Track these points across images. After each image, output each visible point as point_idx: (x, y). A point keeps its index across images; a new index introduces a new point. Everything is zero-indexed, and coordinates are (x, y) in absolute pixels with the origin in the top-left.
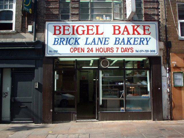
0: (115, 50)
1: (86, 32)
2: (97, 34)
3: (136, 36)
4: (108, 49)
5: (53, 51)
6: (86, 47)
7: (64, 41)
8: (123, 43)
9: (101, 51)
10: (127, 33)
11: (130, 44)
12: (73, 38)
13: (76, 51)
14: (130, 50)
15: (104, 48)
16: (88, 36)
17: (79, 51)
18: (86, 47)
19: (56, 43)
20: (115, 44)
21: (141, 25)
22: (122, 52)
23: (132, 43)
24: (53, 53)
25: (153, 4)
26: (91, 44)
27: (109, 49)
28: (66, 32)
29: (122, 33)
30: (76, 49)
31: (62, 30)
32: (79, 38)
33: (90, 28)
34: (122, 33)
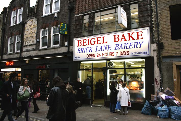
0: (115, 54)
1: (96, 43)
2: (103, 43)
3: (132, 41)
4: (110, 54)
7: (137, 44)
8: (121, 48)
9: (106, 55)
10: (124, 40)
11: (127, 48)
14: (126, 53)
16: (97, 45)
17: (92, 56)
18: (96, 53)
19: (79, 52)
20: (116, 49)
22: (120, 55)
23: (128, 47)
25: (147, 13)
26: (99, 51)
28: (85, 44)
29: (120, 40)
30: (90, 55)
31: (82, 43)
33: (99, 39)
34: (120, 40)
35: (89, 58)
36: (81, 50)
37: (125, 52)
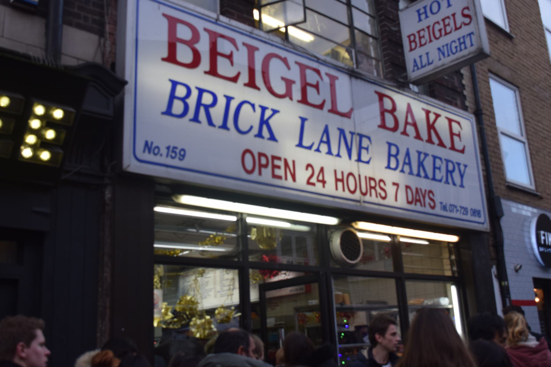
5: (164, 151)
6: (301, 157)
12: (253, 106)
13: (263, 170)
14: (427, 200)
15: (359, 176)
17: (278, 172)
18: (301, 157)
21: (444, 114)
24: (163, 160)
26: (318, 150)
27: (373, 184)
28: (223, 66)
32: (275, 112)
35: (255, 176)
36: (199, 103)
37: (421, 190)
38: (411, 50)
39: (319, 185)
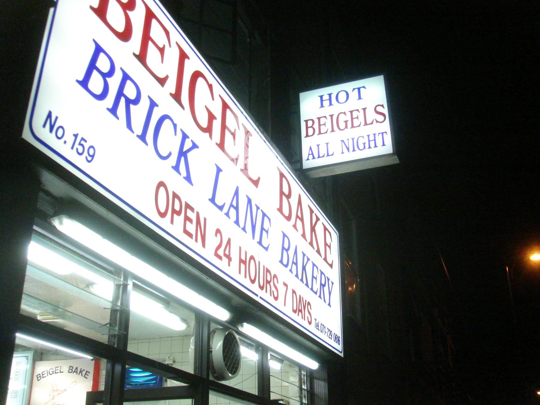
38: (307, 136)
39: (225, 260)
